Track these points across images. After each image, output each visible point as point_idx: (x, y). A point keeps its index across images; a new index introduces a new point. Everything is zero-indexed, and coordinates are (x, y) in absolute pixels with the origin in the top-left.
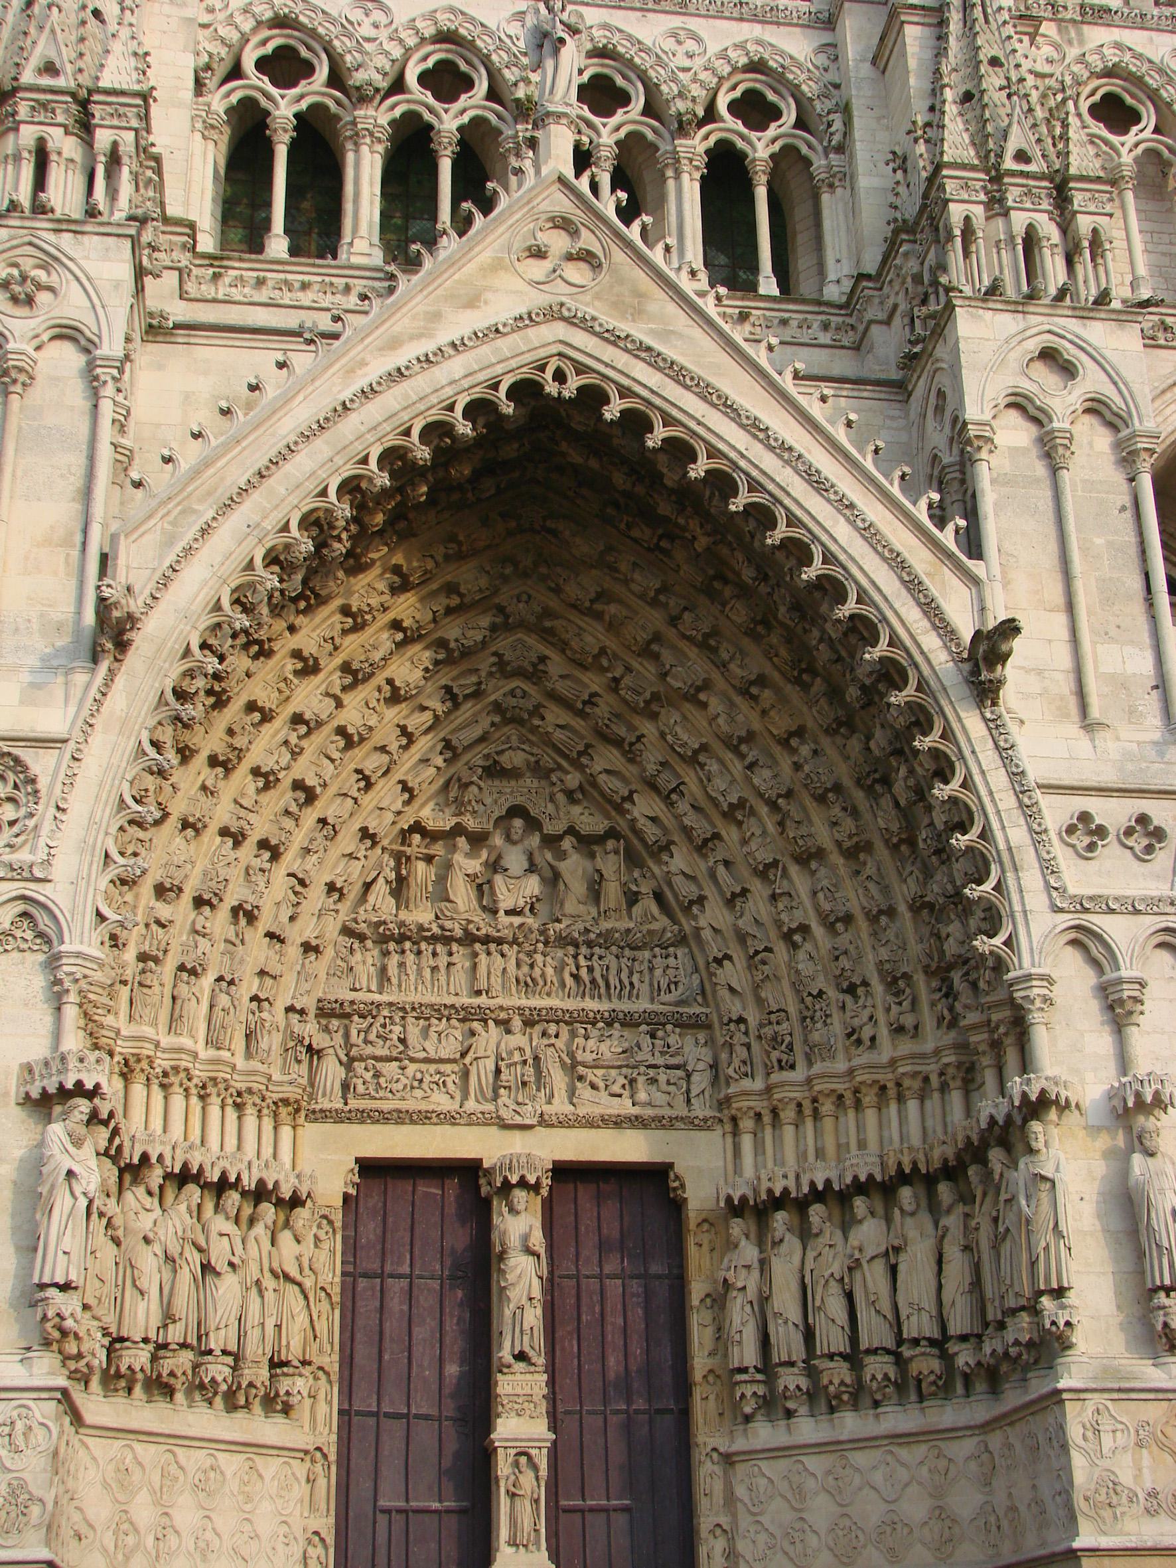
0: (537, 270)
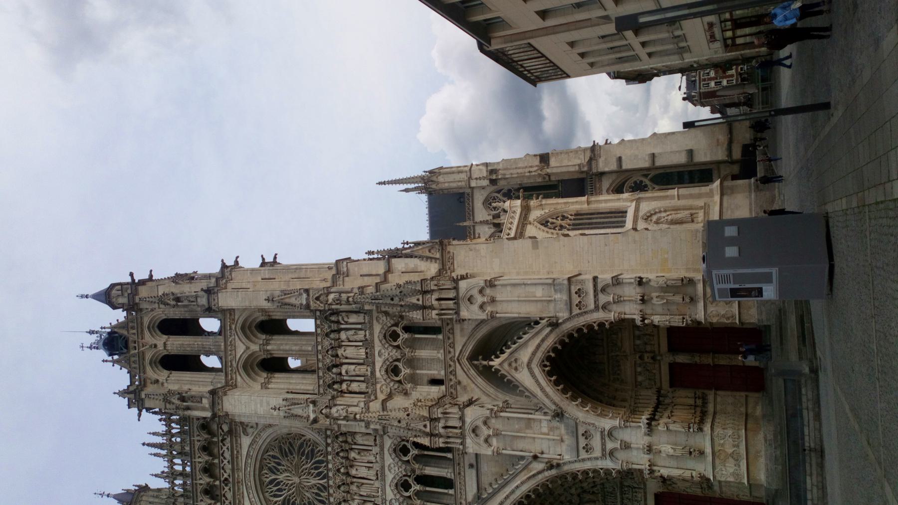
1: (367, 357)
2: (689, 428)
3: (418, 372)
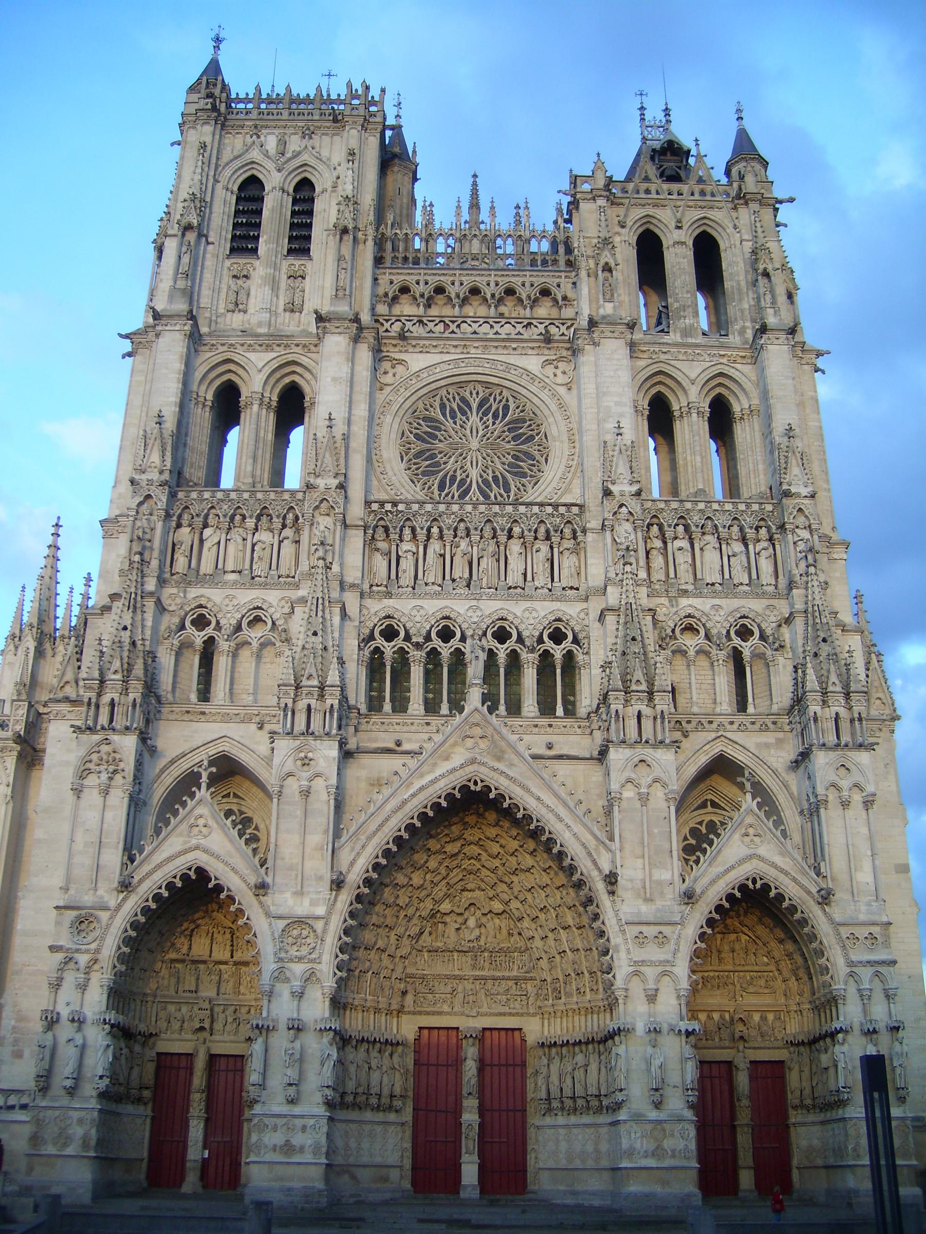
0: (469, 743)
1: (707, 584)
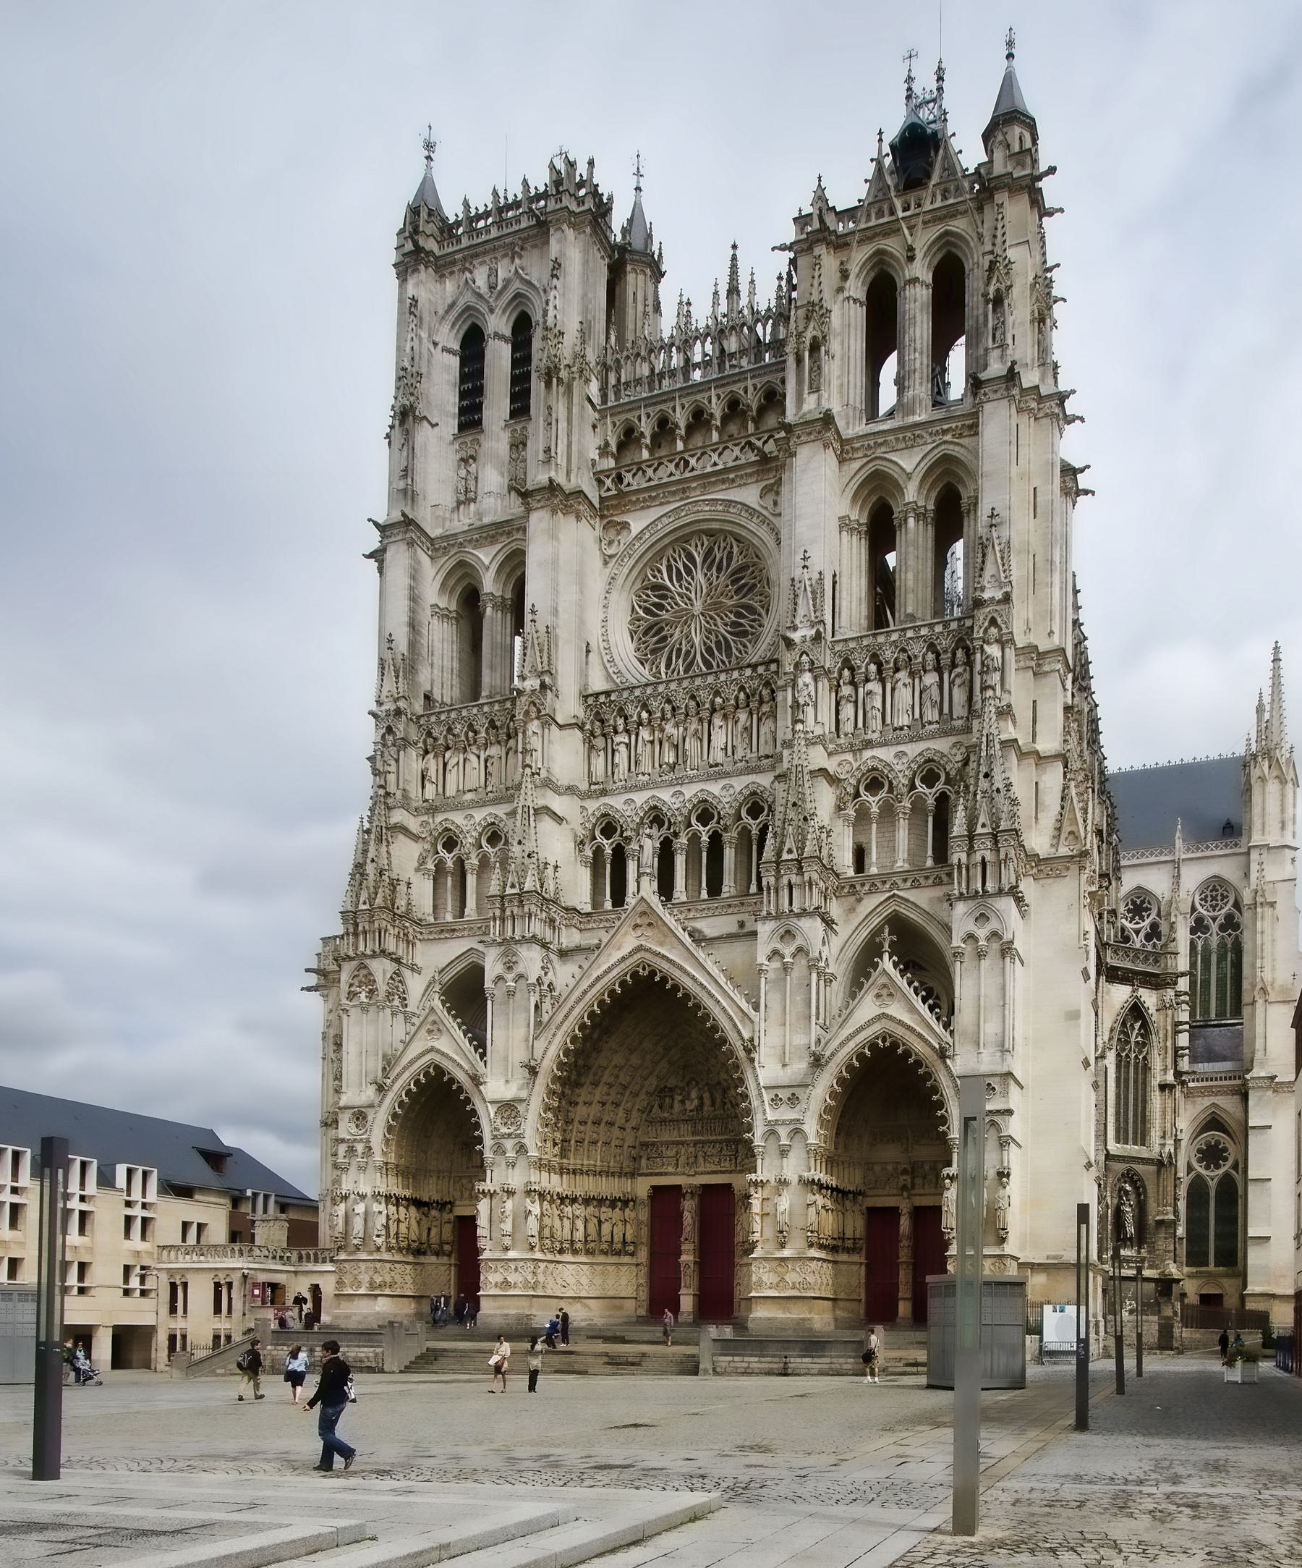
2: (812, 1232)
3: (874, 826)
